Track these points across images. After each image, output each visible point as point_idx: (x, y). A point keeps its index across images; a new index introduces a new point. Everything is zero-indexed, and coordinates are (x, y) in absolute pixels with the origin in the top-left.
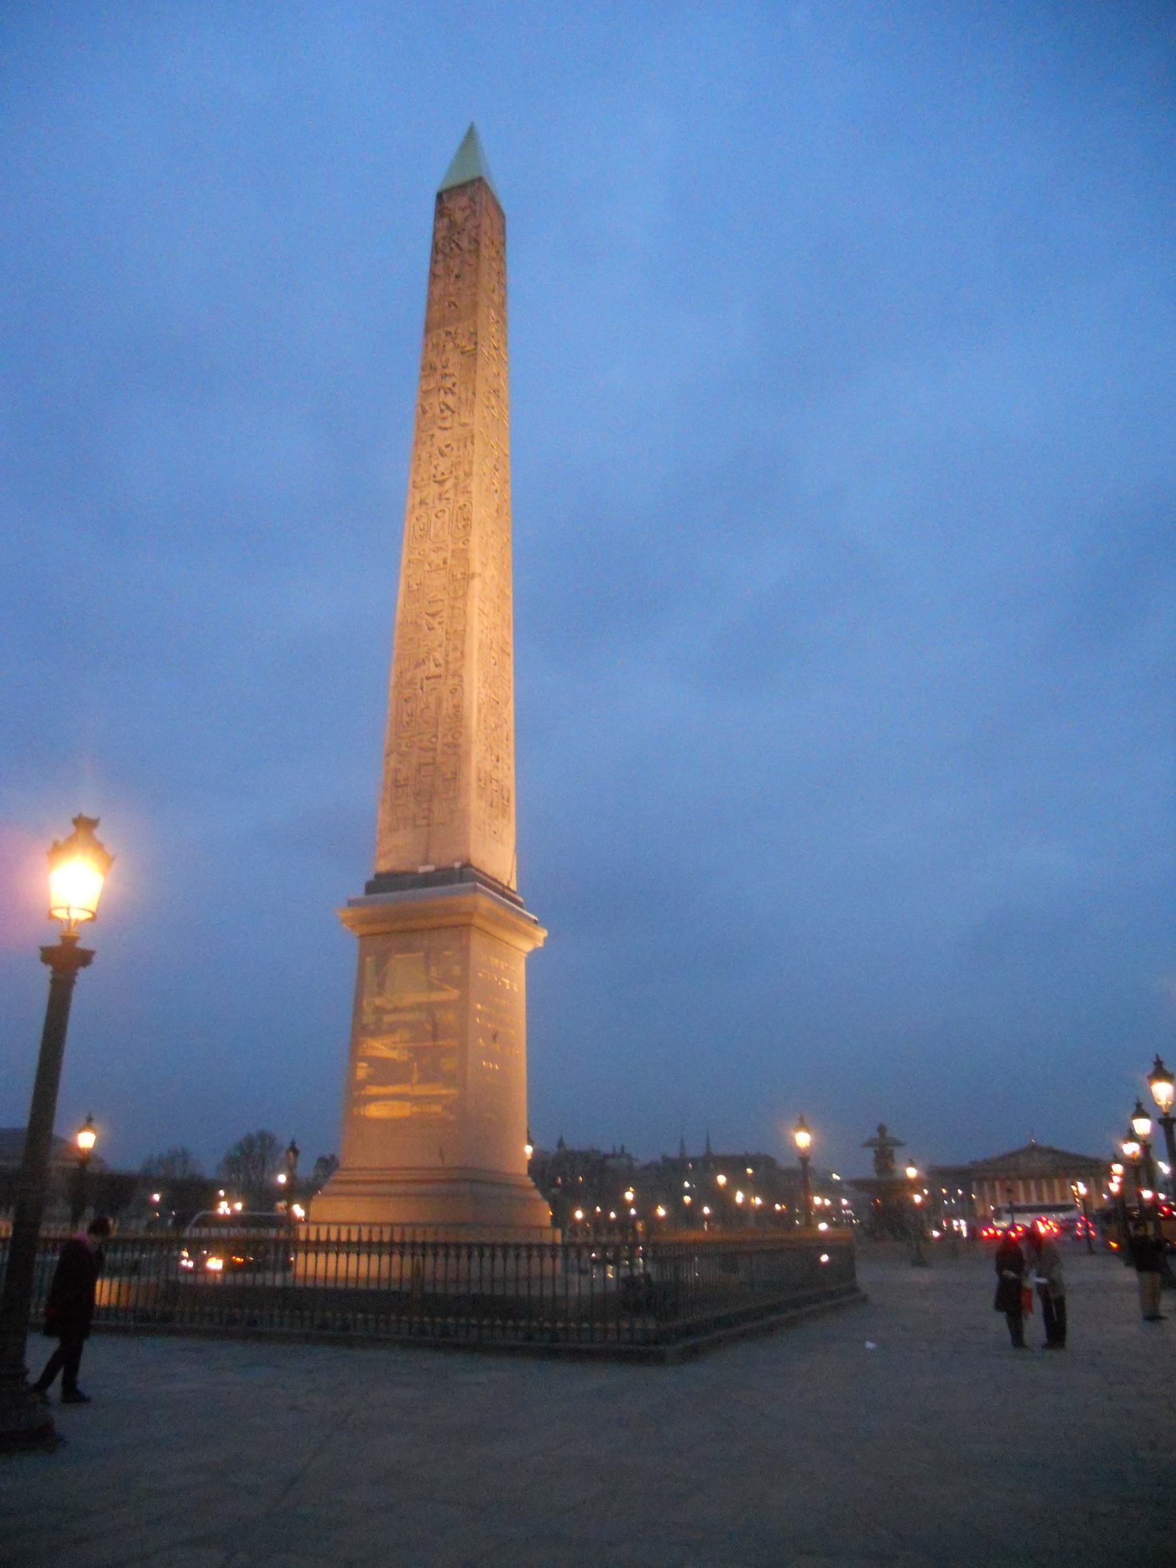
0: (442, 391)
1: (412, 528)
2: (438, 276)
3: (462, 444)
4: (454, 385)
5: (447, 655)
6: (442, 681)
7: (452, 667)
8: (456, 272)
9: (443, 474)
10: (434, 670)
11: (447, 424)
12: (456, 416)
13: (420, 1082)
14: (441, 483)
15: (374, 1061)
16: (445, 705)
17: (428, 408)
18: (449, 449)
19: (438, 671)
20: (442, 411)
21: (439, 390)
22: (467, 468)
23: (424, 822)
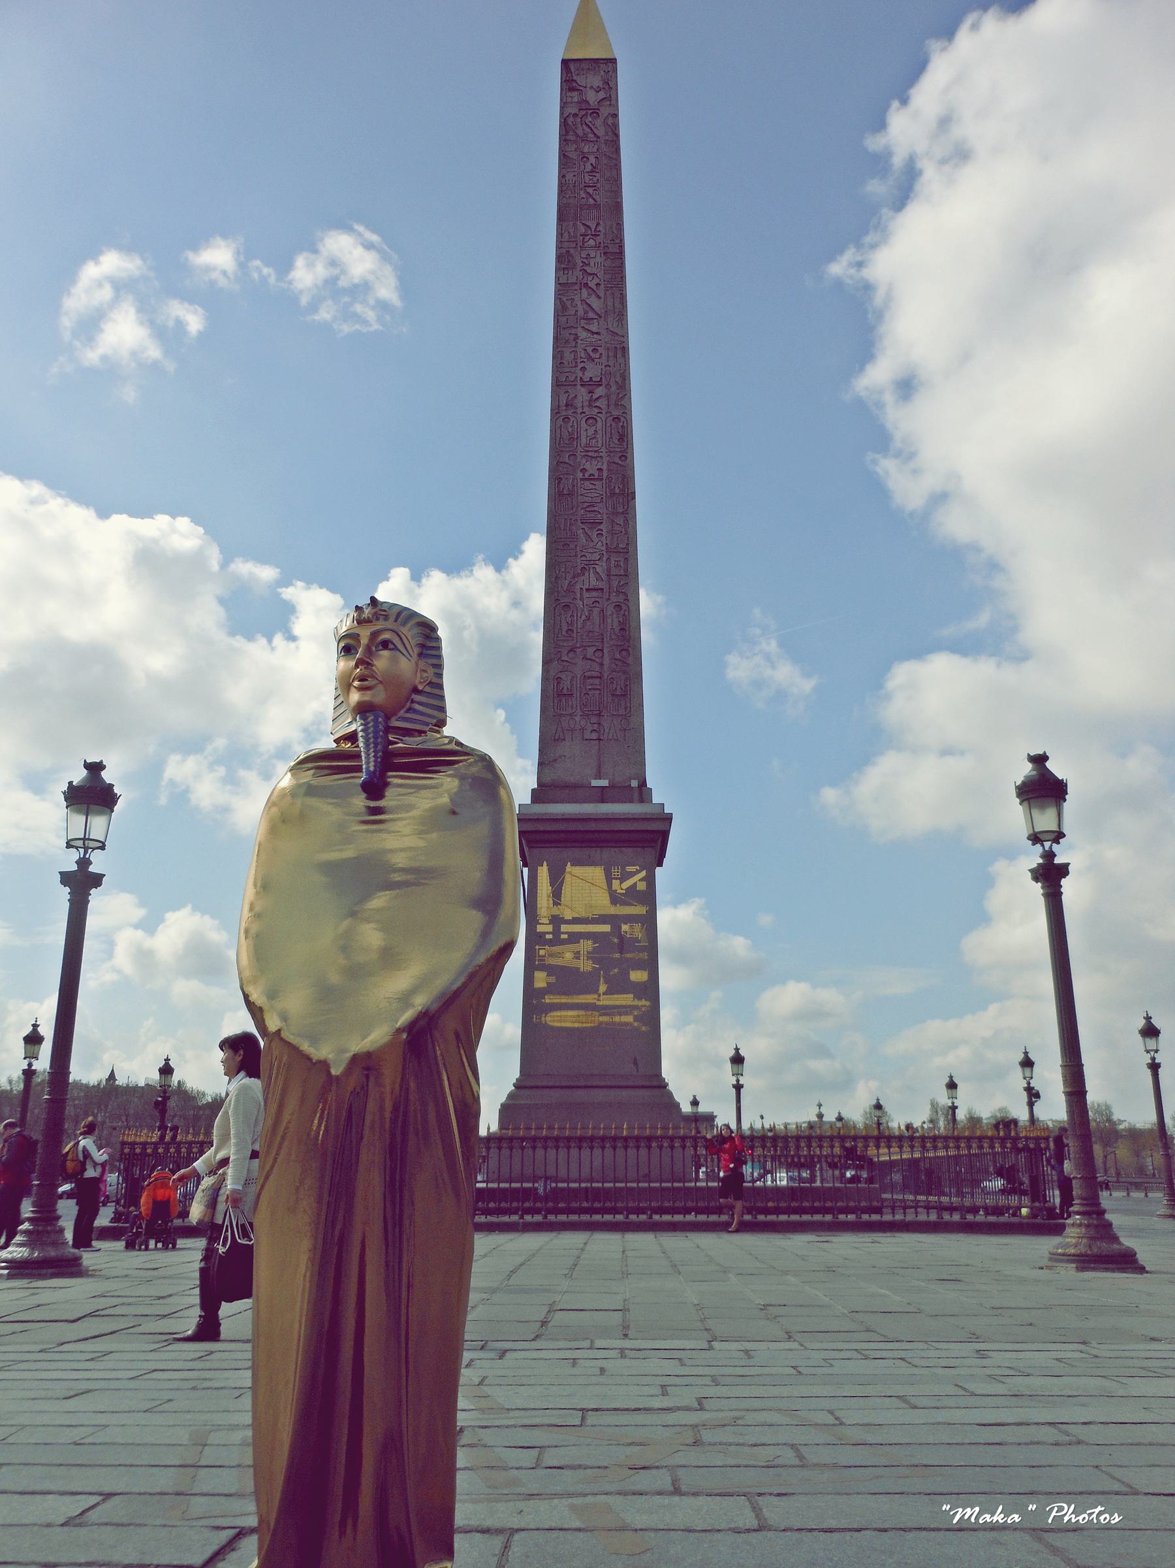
1: (558, 432)
3: (611, 354)
5: (609, 570)
7: (615, 583)
10: (594, 583)
11: (594, 328)
12: (602, 321)
13: (608, 992)
15: (550, 970)
16: (609, 621)
17: (568, 303)
19: (600, 585)
20: (586, 312)
21: (581, 289)
22: (619, 379)
23: (594, 735)
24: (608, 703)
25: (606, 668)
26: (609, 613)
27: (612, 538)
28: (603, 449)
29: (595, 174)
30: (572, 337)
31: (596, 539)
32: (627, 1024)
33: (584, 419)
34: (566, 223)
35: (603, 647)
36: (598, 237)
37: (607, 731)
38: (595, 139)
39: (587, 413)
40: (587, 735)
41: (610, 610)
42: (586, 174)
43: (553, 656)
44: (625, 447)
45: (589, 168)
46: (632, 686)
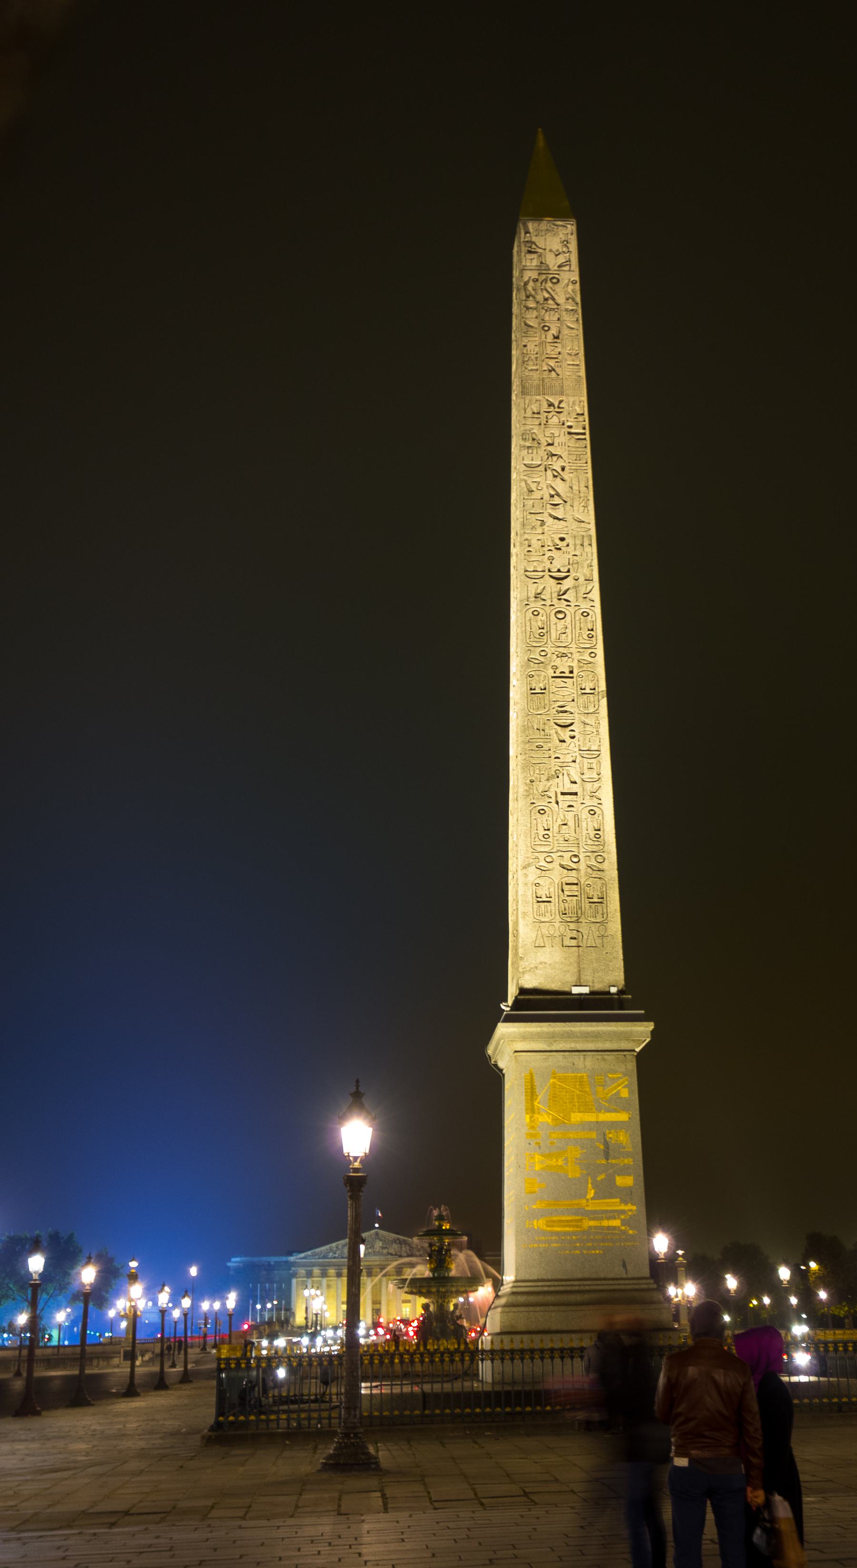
0: (549, 472)
1: (528, 624)
2: (531, 327)
3: (578, 542)
4: (563, 469)
6: (579, 798)
8: (554, 331)
9: (559, 571)
12: (568, 506)
14: (559, 579)
16: (584, 825)
18: (565, 543)
19: (574, 788)
21: (546, 470)
23: (574, 943)
24: (585, 908)
25: (583, 873)
26: (584, 817)
27: (585, 739)
28: (573, 645)
29: (555, 345)
30: (539, 523)
31: (568, 740)
32: (614, 1228)
33: (554, 612)
34: (529, 397)
35: (579, 853)
36: (562, 414)
37: (585, 937)
38: (556, 307)
39: (556, 606)
40: (568, 942)
41: (585, 815)
42: (548, 344)
43: (531, 861)
44: (595, 643)
45: (550, 338)
46: (608, 892)
